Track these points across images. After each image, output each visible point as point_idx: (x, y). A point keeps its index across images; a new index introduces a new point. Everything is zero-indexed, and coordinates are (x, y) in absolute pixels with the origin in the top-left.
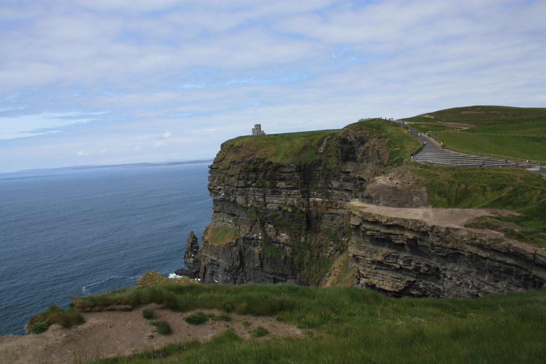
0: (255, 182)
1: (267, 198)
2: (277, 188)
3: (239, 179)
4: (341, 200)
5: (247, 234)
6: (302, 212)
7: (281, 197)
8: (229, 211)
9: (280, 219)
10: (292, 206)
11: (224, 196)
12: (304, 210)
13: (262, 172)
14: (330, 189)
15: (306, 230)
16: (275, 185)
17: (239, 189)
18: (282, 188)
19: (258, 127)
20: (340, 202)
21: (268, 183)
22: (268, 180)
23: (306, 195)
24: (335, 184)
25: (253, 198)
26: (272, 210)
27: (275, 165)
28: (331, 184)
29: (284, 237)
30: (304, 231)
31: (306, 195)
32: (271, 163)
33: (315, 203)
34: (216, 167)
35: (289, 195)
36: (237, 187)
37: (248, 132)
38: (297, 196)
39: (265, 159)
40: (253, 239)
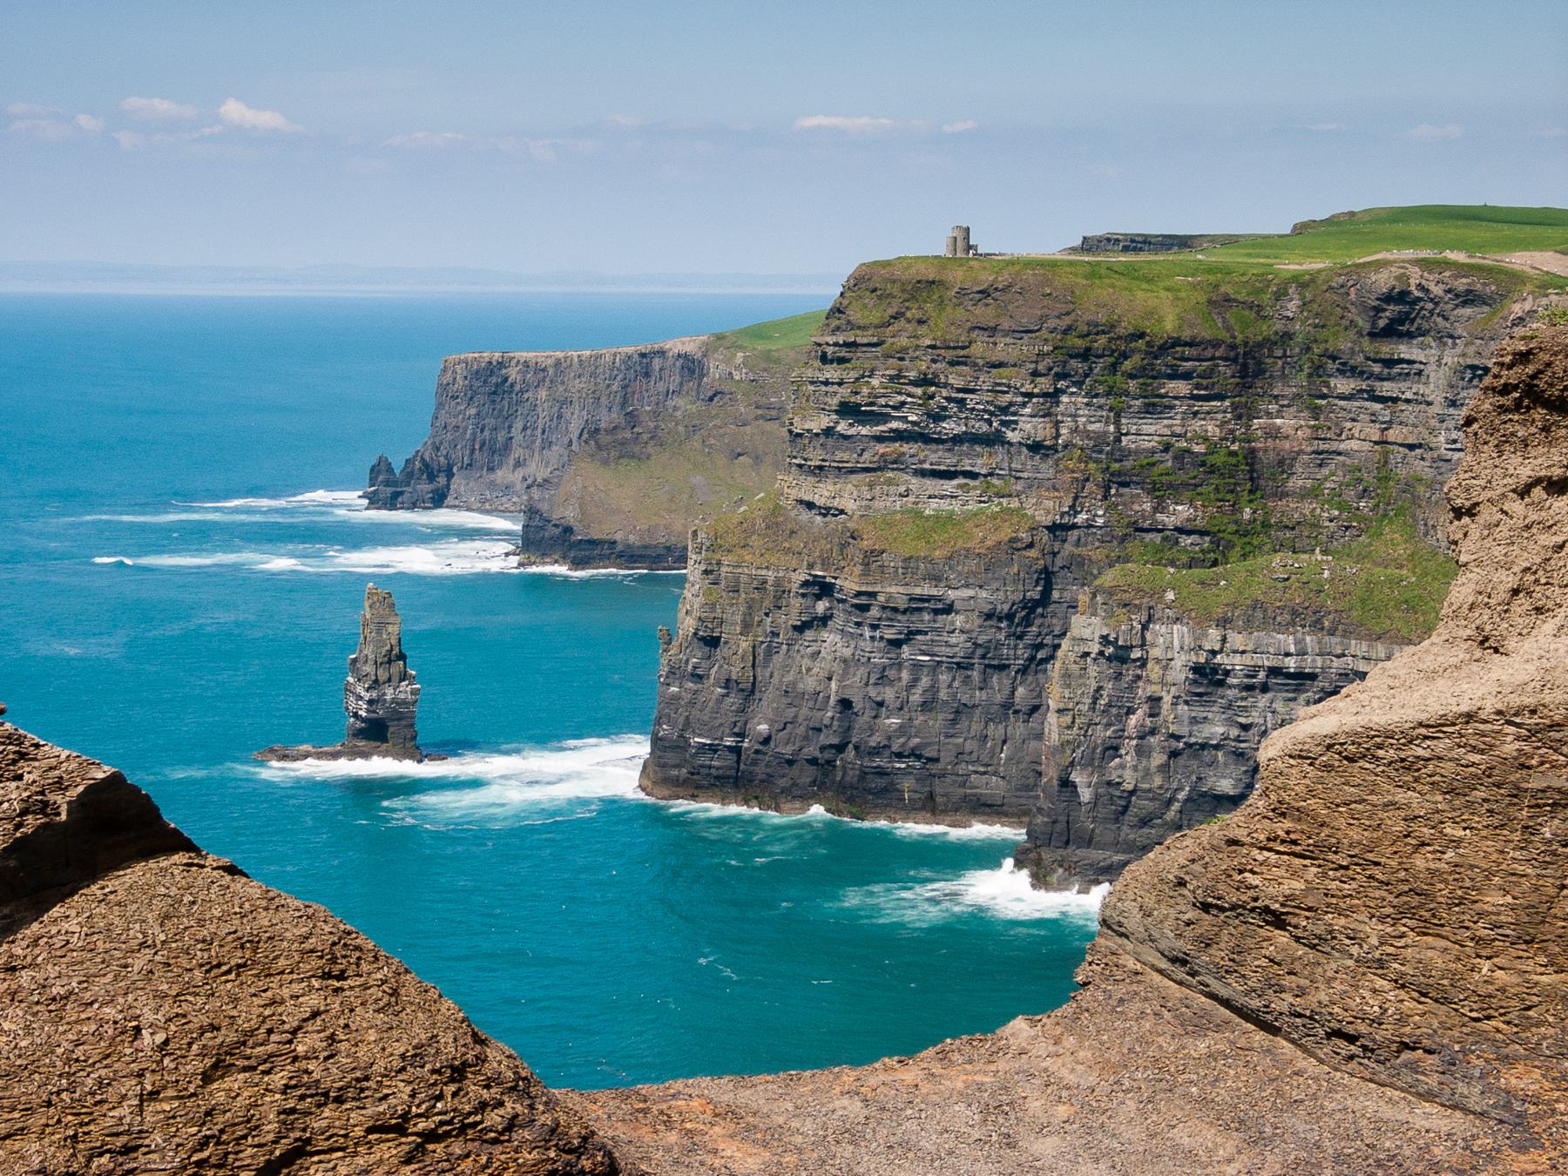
2: (1162, 397)
3: (1035, 374)
4: (1354, 420)
5: (1063, 515)
12: (1235, 447)
13: (1102, 356)
14: (1324, 397)
15: (1251, 492)
18: (1176, 398)
20: (1348, 425)
21: (1132, 385)
22: (1132, 376)
23: (1244, 413)
24: (1343, 385)
26: (1137, 452)
32: (1142, 335)
33: (1274, 434)
34: (875, 340)
35: (1195, 414)
38: (1220, 416)
40: (1074, 526)
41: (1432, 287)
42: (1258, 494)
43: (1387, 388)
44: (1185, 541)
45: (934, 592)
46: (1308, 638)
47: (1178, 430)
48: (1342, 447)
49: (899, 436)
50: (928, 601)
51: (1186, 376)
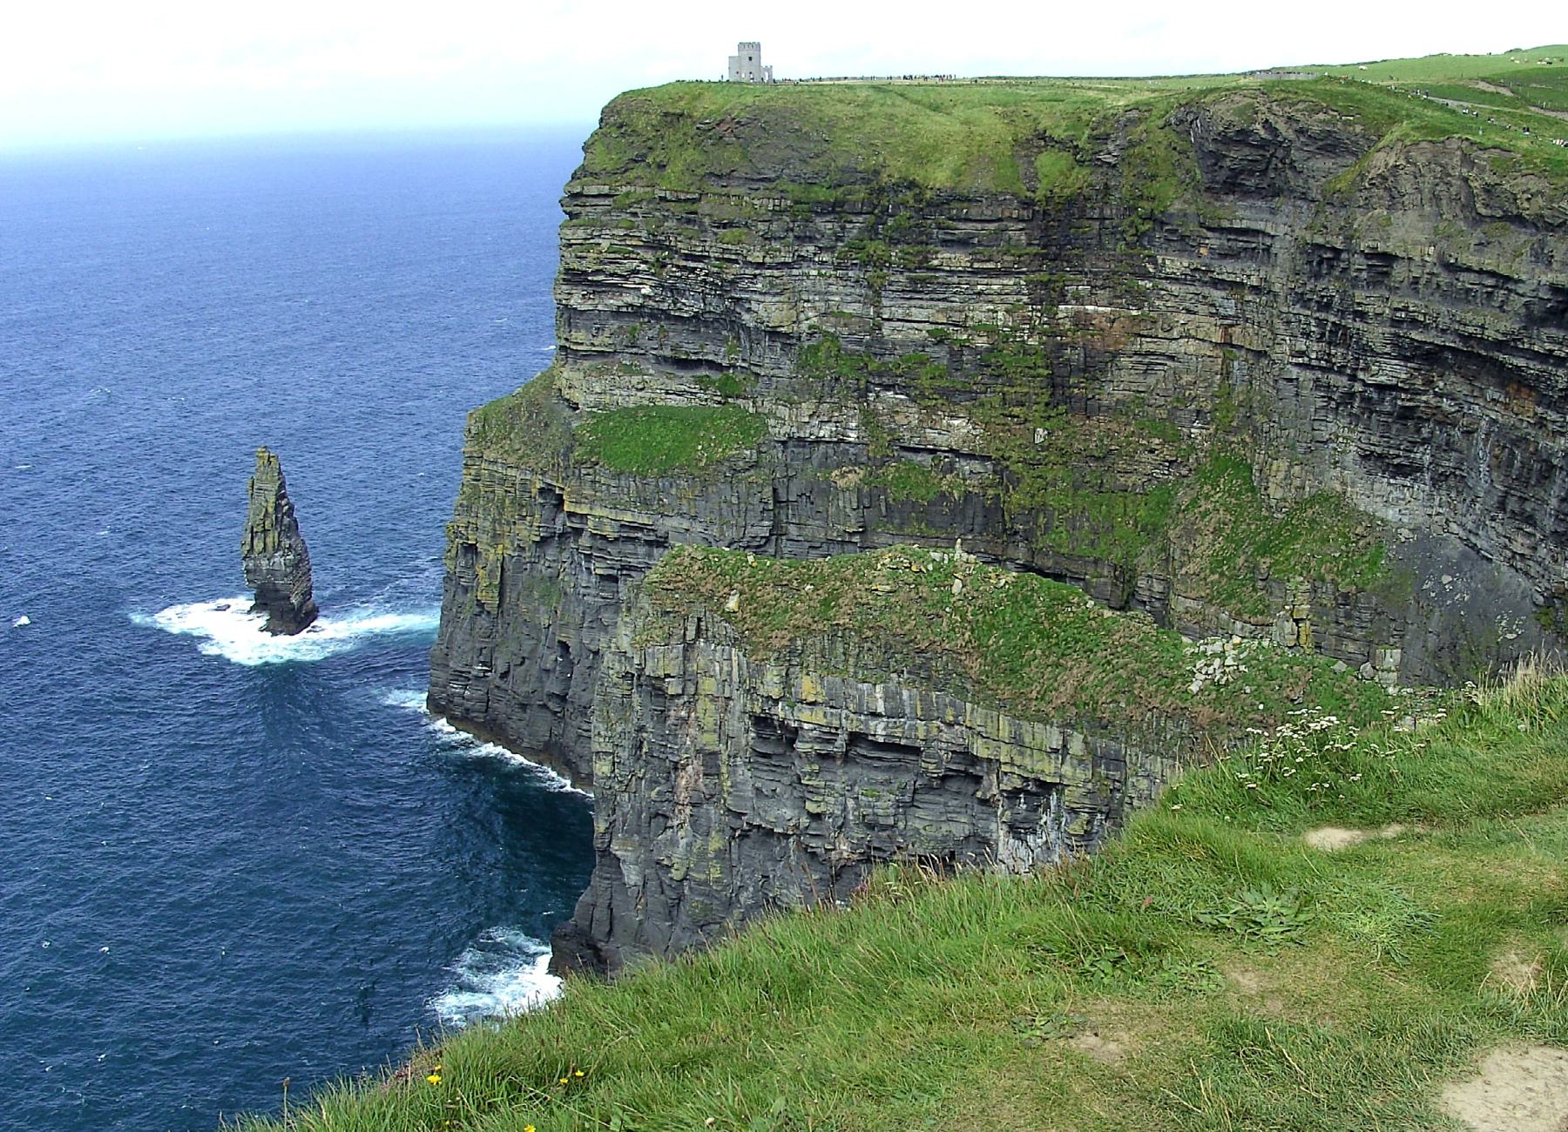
0: (831, 249)
1: (885, 302)
2: (935, 269)
4: (1189, 311)
6: (1025, 350)
7: (944, 300)
8: (667, 353)
9: (961, 372)
10: (991, 331)
11: (645, 296)
12: (1031, 342)
14: (1146, 276)
16: (926, 260)
17: (768, 272)
19: (751, 51)
20: (1182, 318)
23: (1049, 295)
24: (1176, 264)
25: (821, 305)
27: (929, 194)
28: (1155, 263)
29: (958, 429)
30: (1042, 407)
31: (1049, 295)
33: (1082, 322)
34: (606, 190)
36: (761, 265)
37: (714, 69)
38: (1012, 299)
39: (876, 173)
41: (1281, 126)
42: (1062, 408)
43: (1228, 270)
44: (966, 466)
45: (644, 520)
46: (905, 694)
47: (957, 317)
48: (1173, 347)
49: (637, 311)
50: (641, 530)
51: (964, 243)
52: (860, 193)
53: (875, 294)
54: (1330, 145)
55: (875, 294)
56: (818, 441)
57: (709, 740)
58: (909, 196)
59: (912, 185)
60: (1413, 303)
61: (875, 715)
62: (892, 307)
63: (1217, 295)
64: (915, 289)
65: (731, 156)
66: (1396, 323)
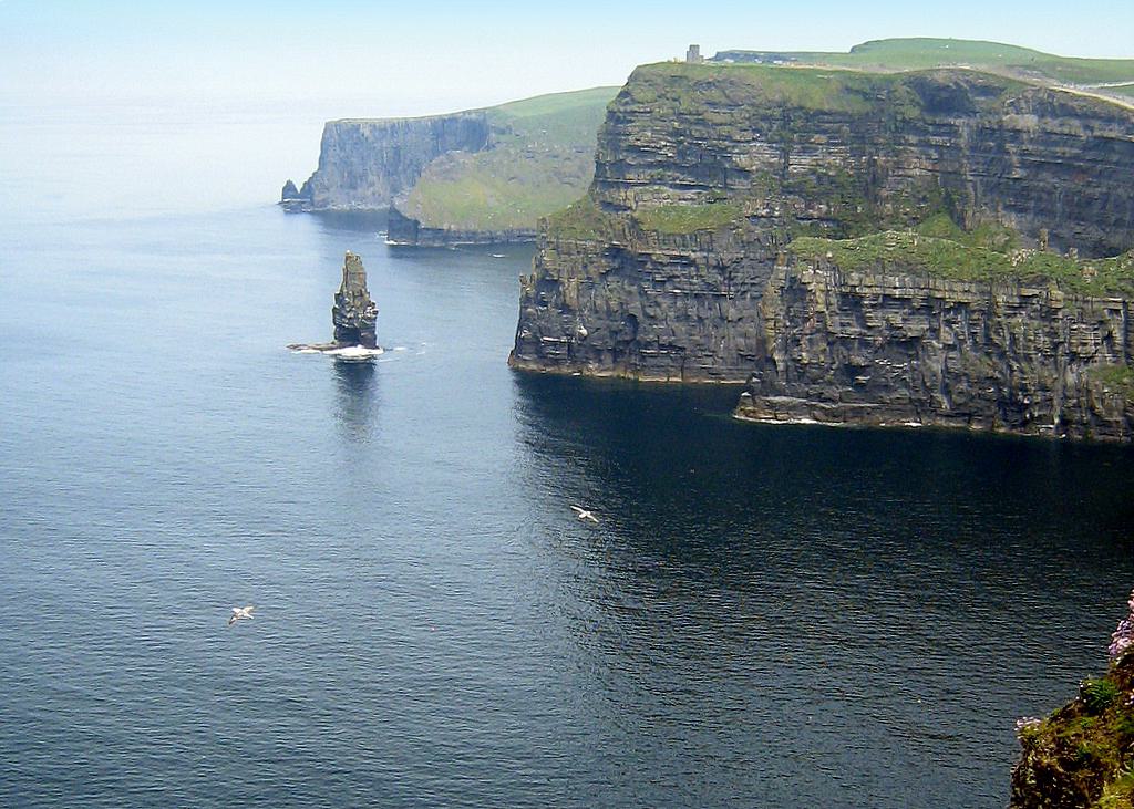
2: (812, 143)
14: (900, 144)
24: (913, 139)
39: (785, 103)
51: (824, 132)
52: (777, 113)
53: (786, 153)
54: (987, 91)
55: (786, 153)
56: (762, 216)
57: (821, 308)
58: (800, 113)
59: (801, 108)
60: (1030, 147)
61: (895, 288)
62: (793, 159)
63: (932, 151)
64: (804, 151)
65: (715, 94)
66: (1021, 155)
